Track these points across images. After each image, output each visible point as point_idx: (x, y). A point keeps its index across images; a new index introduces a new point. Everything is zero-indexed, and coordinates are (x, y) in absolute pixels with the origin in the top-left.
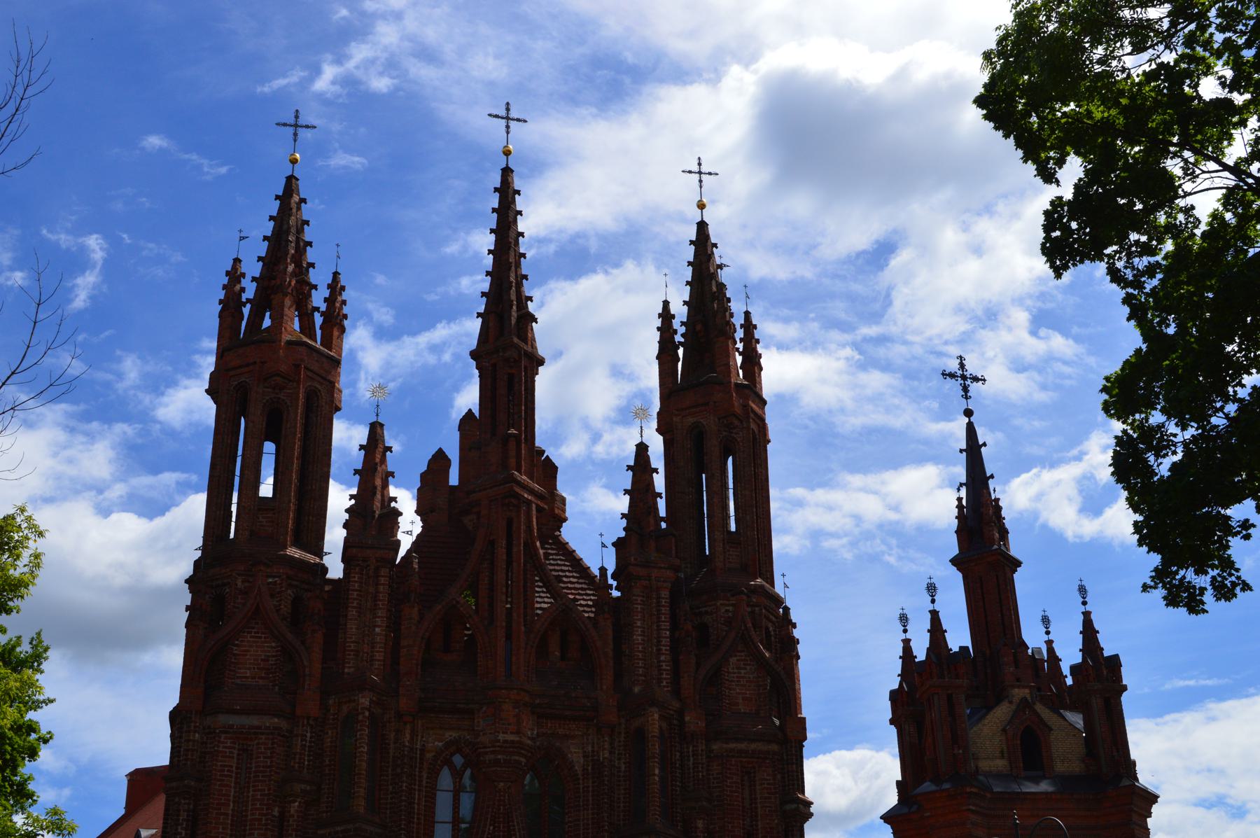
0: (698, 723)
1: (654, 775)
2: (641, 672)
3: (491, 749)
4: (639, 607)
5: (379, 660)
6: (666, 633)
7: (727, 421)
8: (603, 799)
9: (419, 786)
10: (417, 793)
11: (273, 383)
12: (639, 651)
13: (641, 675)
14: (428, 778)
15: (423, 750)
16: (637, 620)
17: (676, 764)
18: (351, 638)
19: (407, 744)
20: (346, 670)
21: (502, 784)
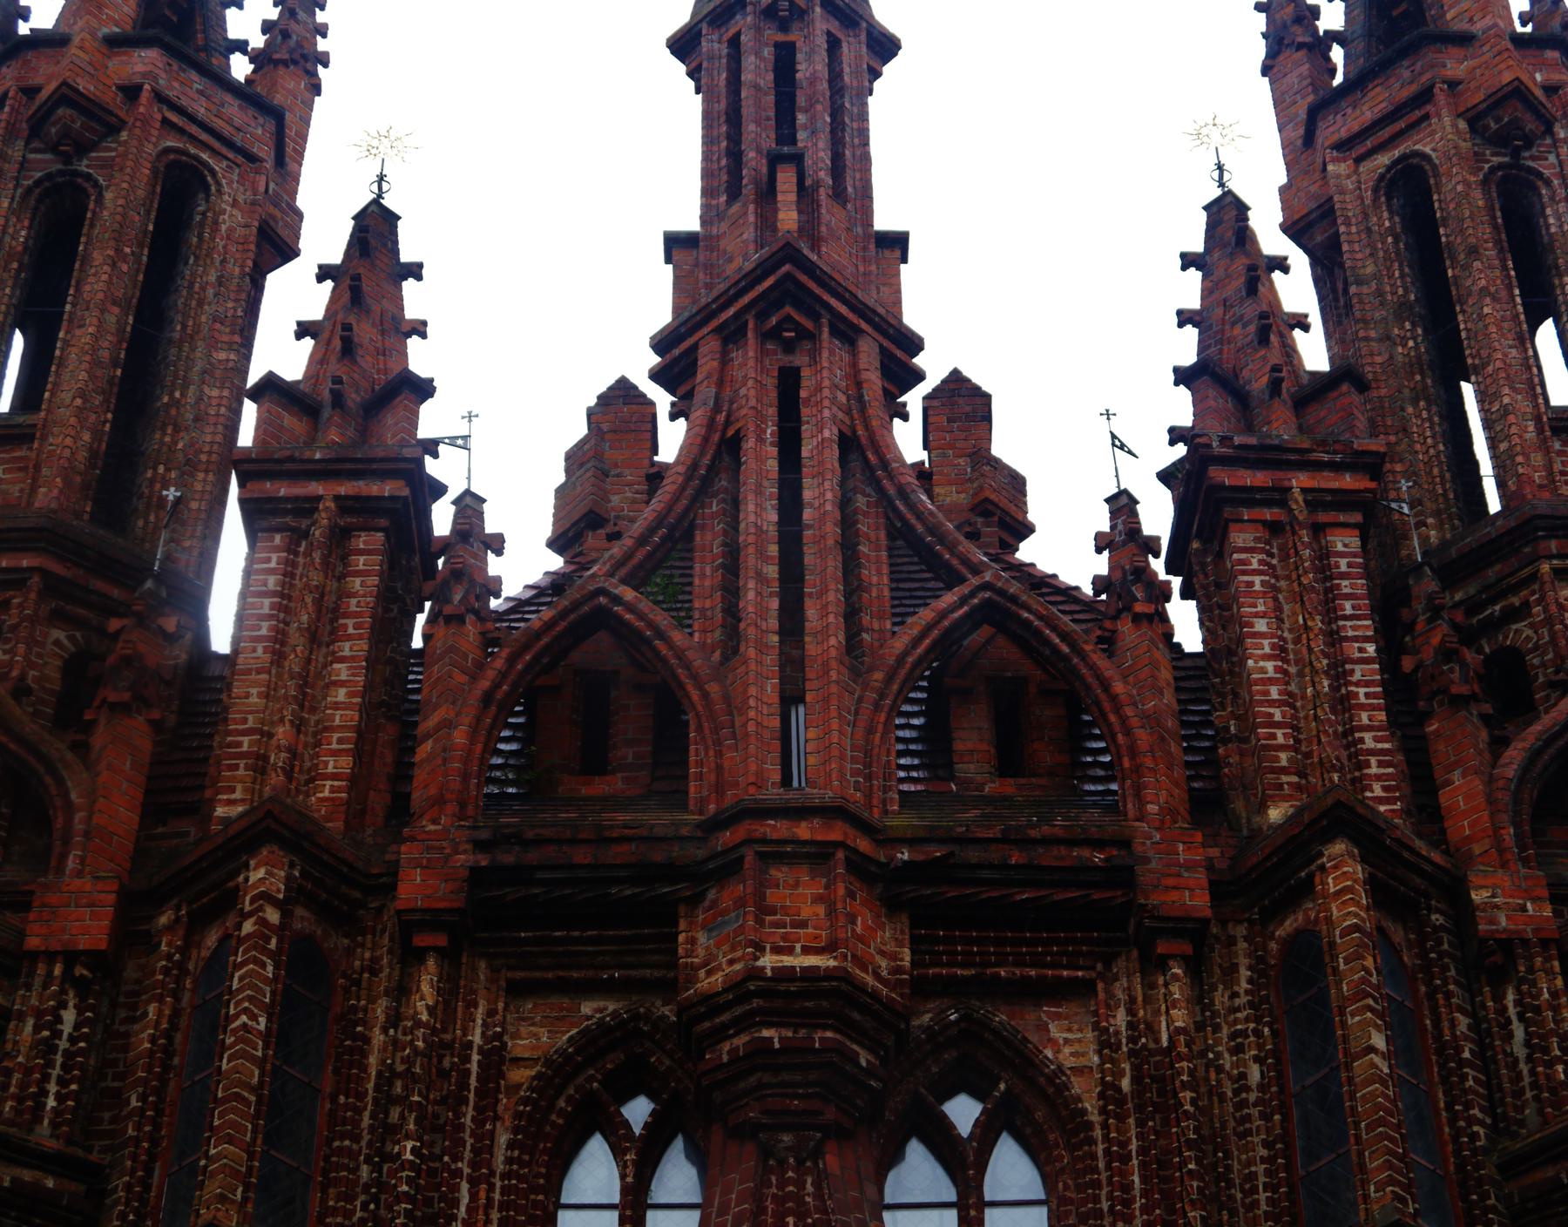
0: (1524, 909)
1: (1372, 1049)
2: (1284, 763)
3: (738, 1011)
4: (1257, 580)
5: (335, 777)
6: (1361, 650)
7: (1498, 120)
8: (1184, 1163)
9: (474, 1165)
10: (465, 1187)
11: (53, 130)
12: (1272, 703)
13: (1284, 770)
14: (511, 1145)
15: (496, 1059)
16: (1257, 615)
17: (1459, 1050)
18: (245, 721)
19: (425, 1017)
20: (220, 811)
21: (787, 1138)
